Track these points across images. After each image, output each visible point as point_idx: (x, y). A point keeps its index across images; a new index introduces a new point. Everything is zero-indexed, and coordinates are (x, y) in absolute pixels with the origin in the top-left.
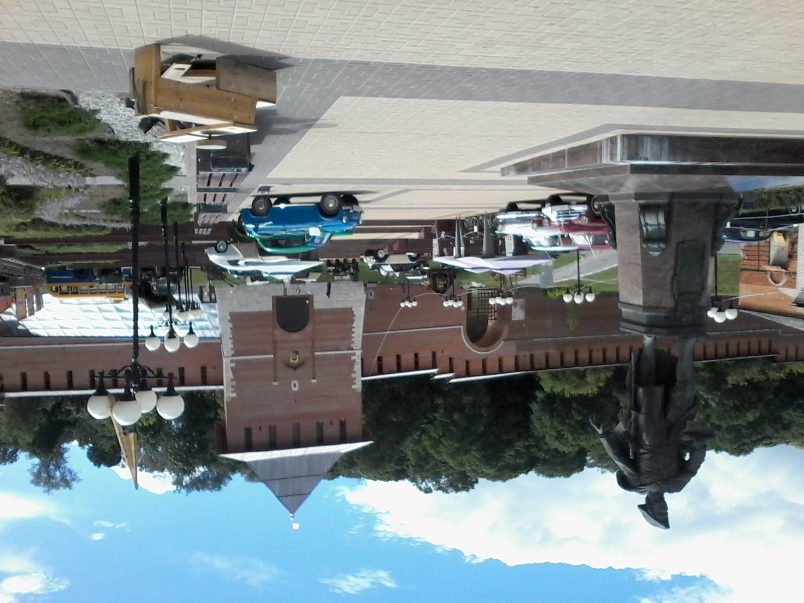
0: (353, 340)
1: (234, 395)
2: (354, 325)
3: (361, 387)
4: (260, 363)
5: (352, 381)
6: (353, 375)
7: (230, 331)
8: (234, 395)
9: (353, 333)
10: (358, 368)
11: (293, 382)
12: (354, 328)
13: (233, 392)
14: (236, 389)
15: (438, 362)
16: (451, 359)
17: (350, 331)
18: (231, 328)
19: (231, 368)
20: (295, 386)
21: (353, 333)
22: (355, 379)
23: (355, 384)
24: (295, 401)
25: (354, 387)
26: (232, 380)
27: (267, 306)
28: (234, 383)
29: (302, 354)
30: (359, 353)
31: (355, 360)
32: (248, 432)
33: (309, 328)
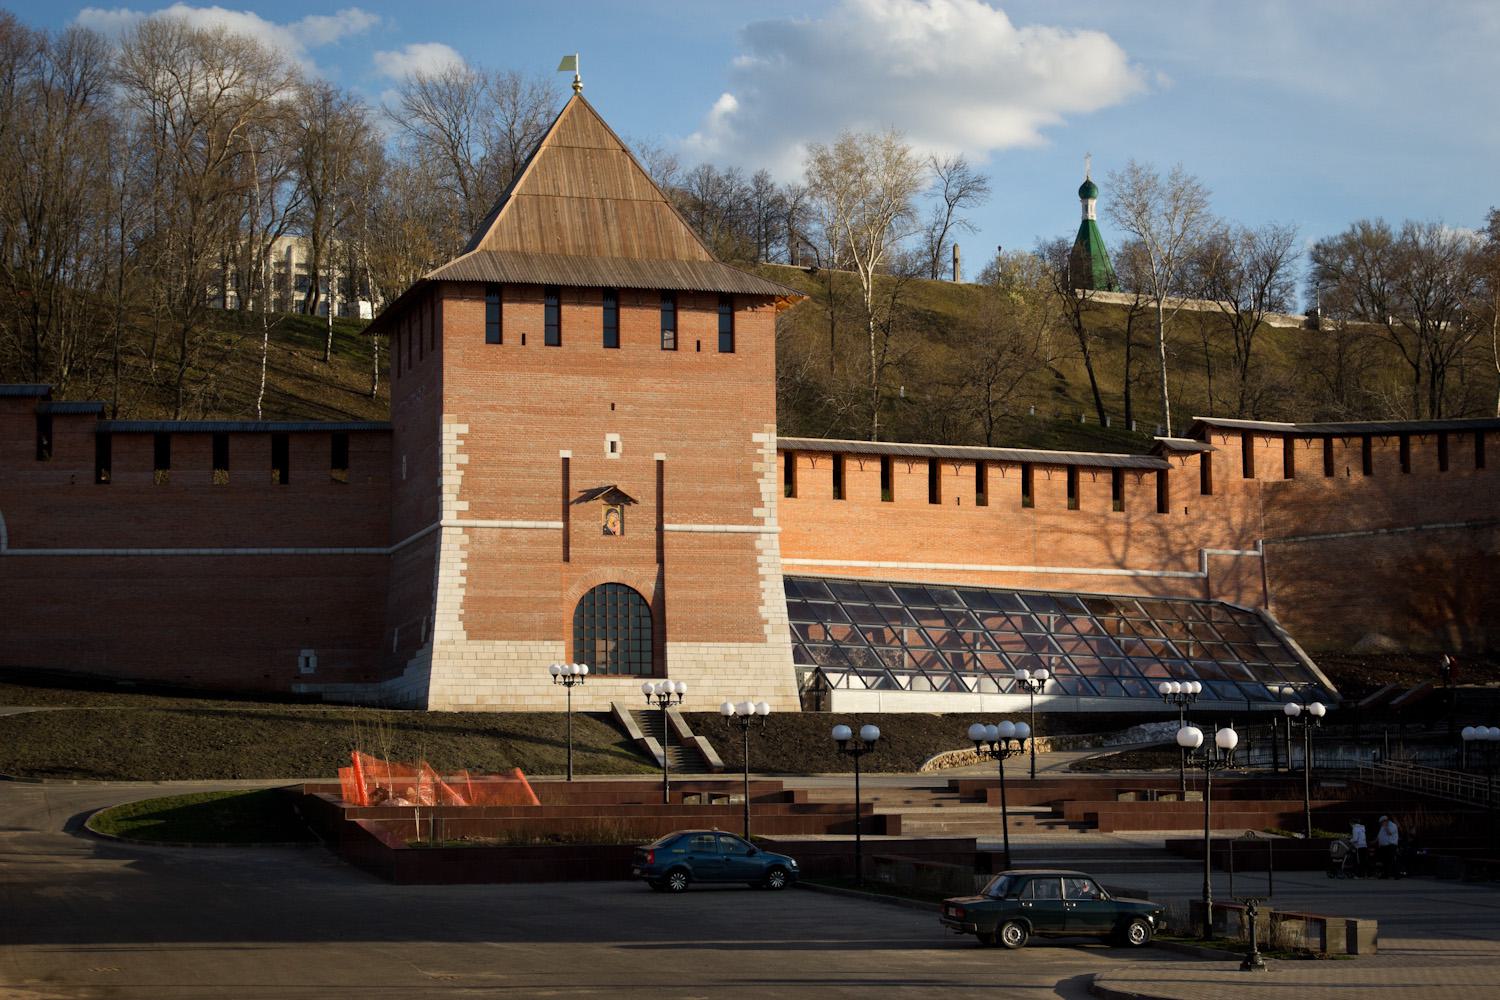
0: (464, 554)
1: (757, 437)
2: (462, 592)
3: (445, 427)
4: (694, 513)
5: (468, 445)
6: (464, 459)
7: (764, 596)
8: (757, 437)
9: (463, 573)
10: (451, 479)
11: (615, 456)
12: (461, 586)
13: (760, 445)
14: (752, 452)
15: (91, 450)
16: (43, 452)
17: (472, 578)
18: (762, 603)
19: (761, 504)
20: (613, 445)
21: (463, 573)
22: (460, 450)
23: (460, 437)
24: (613, 406)
25: (464, 429)
26: (761, 475)
27: (676, 652)
28: (757, 467)
29: (596, 527)
30: (448, 517)
31: (460, 498)
32: (727, 343)
33: (575, 593)
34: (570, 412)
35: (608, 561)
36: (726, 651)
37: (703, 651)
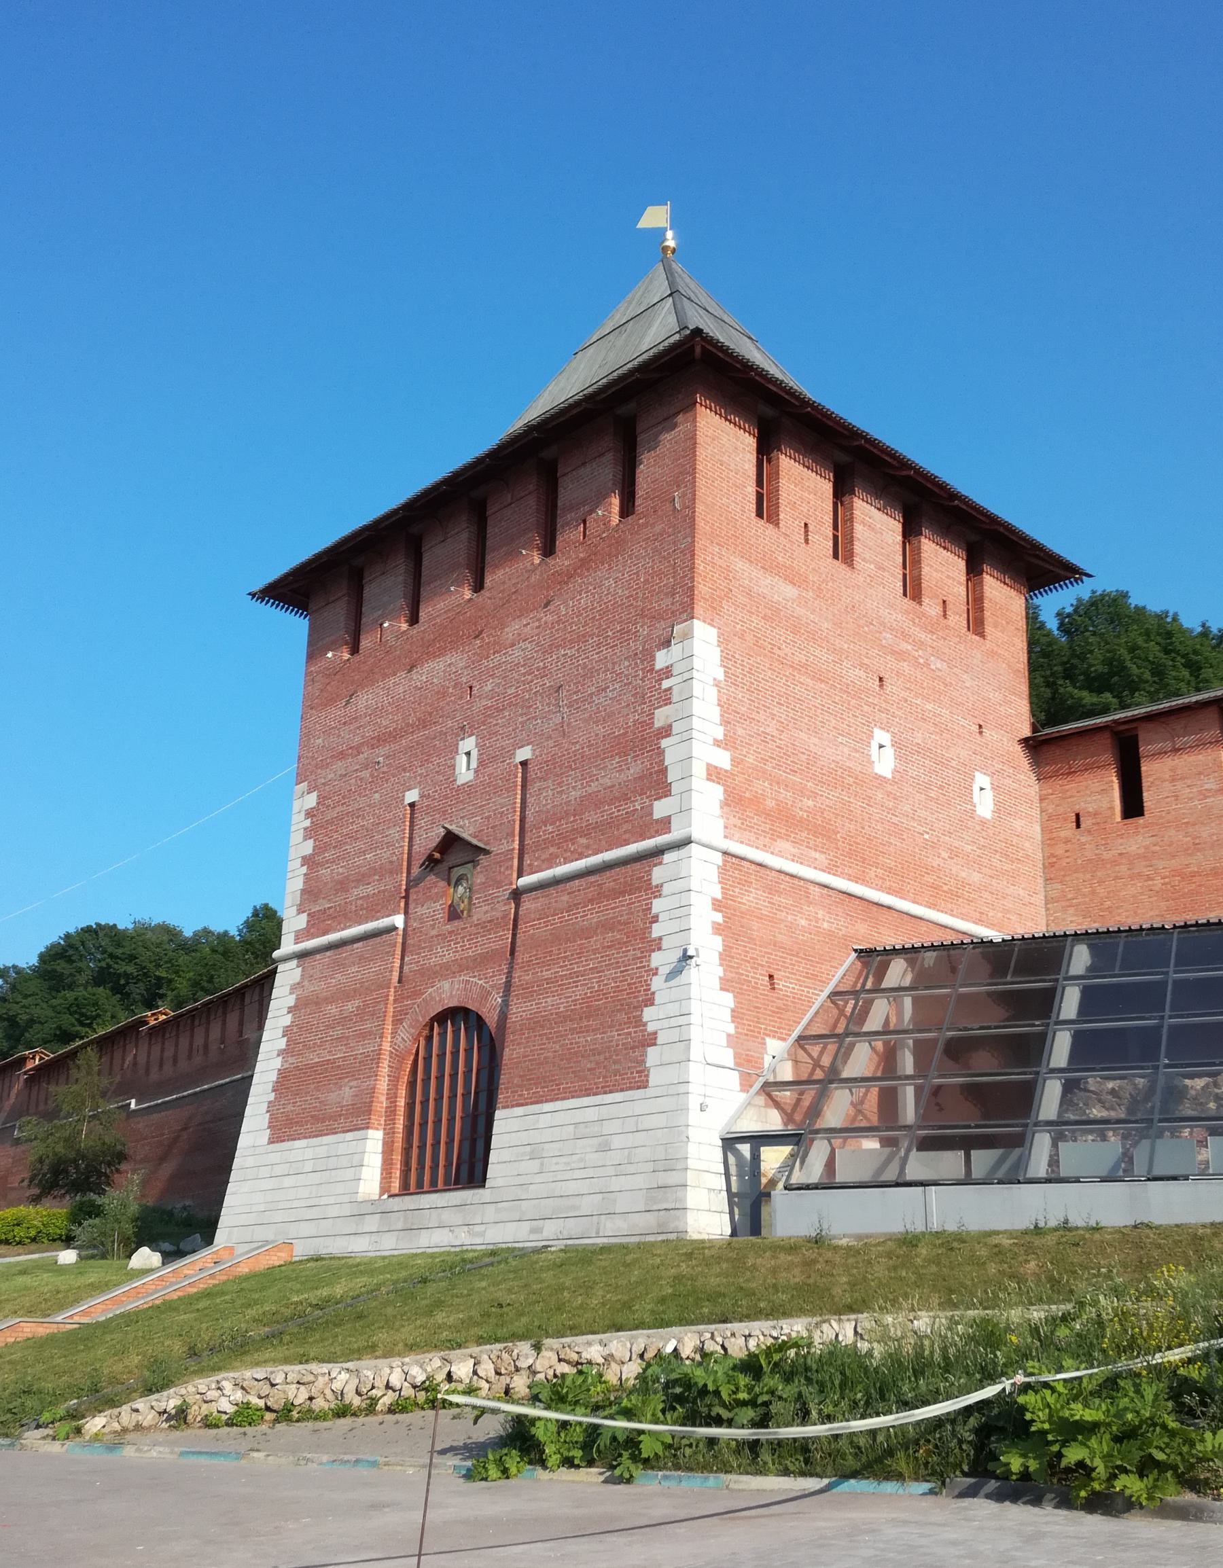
28: (661, 717)
34: (423, 724)
35: (446, 971)
36: (579, 1116)
37: (544, 1120)
